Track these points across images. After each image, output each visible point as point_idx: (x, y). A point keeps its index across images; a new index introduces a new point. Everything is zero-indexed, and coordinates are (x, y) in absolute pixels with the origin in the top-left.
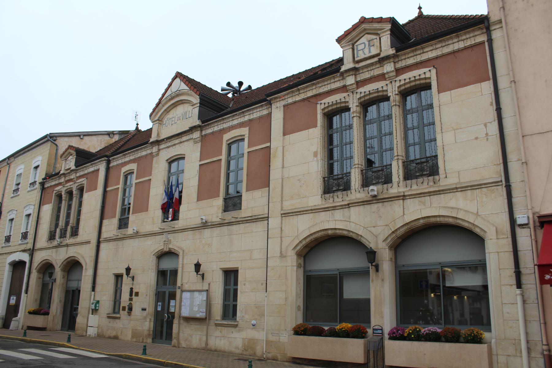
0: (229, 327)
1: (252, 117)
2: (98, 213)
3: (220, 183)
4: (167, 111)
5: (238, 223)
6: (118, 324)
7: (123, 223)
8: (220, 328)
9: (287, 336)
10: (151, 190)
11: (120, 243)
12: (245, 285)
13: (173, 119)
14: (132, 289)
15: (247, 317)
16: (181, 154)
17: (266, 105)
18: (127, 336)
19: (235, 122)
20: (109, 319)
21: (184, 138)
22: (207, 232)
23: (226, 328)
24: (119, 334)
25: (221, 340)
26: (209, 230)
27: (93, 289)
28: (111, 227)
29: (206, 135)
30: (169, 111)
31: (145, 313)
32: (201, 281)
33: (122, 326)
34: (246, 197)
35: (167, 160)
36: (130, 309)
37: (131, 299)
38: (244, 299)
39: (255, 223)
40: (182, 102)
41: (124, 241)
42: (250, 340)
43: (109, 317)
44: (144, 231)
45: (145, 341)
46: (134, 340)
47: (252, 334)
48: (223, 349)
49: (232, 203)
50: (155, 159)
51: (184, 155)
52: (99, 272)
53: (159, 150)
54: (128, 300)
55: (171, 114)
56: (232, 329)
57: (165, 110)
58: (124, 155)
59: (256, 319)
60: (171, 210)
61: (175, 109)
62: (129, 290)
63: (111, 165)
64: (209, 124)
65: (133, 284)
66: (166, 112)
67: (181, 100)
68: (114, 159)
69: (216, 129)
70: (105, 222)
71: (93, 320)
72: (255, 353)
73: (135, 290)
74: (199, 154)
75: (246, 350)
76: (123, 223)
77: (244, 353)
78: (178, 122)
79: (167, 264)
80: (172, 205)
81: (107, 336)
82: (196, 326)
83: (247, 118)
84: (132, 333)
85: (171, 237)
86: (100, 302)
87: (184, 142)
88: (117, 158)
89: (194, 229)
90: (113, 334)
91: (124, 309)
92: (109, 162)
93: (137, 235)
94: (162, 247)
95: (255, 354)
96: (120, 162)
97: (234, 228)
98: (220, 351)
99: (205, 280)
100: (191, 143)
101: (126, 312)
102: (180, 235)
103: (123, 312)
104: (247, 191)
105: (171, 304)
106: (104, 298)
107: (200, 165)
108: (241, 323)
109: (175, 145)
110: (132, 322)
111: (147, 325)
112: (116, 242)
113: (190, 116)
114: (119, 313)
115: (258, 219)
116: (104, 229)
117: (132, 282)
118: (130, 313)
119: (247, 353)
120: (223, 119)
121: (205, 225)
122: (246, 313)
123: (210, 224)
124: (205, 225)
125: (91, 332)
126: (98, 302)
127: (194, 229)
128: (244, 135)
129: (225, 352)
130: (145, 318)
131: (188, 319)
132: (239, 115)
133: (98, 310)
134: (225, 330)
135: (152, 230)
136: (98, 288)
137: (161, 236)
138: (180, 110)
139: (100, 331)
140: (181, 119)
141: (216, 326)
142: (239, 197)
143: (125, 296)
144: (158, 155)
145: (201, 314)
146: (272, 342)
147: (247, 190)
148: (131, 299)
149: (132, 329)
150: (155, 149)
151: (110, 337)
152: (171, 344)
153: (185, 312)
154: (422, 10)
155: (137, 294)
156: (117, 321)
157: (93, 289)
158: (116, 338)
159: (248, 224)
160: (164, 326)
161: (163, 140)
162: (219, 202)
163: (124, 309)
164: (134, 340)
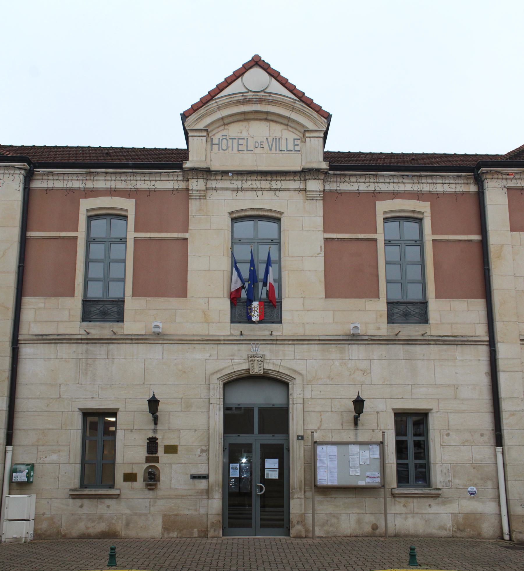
0: (424, 498)
1: (439, 188)
2: (11, 280)
3: (377, 276)
4: (225, 122)
5: (427, 342)
7: (103, 310)
8: (402, 500)
11: (100, 350)
13: (241, 142)
15: (457, 481)
16: (271, 211)
17: (467, 179)
18: (155, 529)
19: (409, 187)
20: (79, 502)
22: (357, 352)
23: (415, 500)
24: (119, 527)
25: (406, 518)
26: (362, 347)
27: (9, 440)
28: (55, 313)
29: (331, 191)
30: (228, 124)
31: (202, 484)
32: (352, 427)
33: (128, 511)
34: (436, 307)
35: (231, 213)
36: (152, 478)
38: (444, 454)
39: (459, 347)
40: (266, 117)
41: (111, 346)
43: (74, 497)
44: (180, 332)
45: (211, 533)
46: (175, 534)
47: (470, 506)
48: (412, 531)
49: (408, 311)
50: (194, 205)
51: (281, 213)
52: (21, 404)
53: (207, 189)
54: (144, 460)
55: (234, 130)
56: (430, 501)
57: (222, 118)
59: (475, 485)
60: (255, 304)
61: (245, 124)
62: (145, 443)
63: (36, 184)
64: (346, 175)
65: (155, 431)
66: (221, 123)
67: (267, 113)
68: (49, 173)
69: (363, 187)
70: (28, 301)
72: (479, 534)
74: (319, 221)
75: (462, 531)
76: (103, 310)
77: (459, 534)
78: (258, 151)
80: (255, 296)
82: (346, 500)
83: (426, 188)
84: (163, 522)
85: (263, 350)
86: (36, 467)
88: (58, 174)
89: (324, 342)
90: (101, 527)
91: (130, 477)
92: (29, 177)
93: (157, 338)
94: (245, 366)
95: (479, 535)
96: (77, 185)
97: (418, 349)
98: (406, 536)
99: (360, 427)
100: (299, 197)
101: (140, 482)
102: (289, 349)
104: (438, 296)
105: (267, 466)
107: (326, 240)
108: (445, 491)
110: (161, 503)
111: (216, 504)
112: (85, 347)
113: (291, 147)
115: (468, 341)
116: (27, 315)
117: (153, 426)
118: (155, 485)
119: (464, 534)
121: (354, 339)
122: (454, 476)
123: (367, 338)
124: (354, 339)
126: (31, 467)
127: (324, 342)
128: (422, 213)
129: (417, 536)
130: (208, 492)
131: (327, 491)
132: (411, 179)
133: (32, 482)
134: (414, 504)
135: (207, 333)
136: (19, 437)
137: (235, 347)
138: (259, 130)
139: (44, 526)
140: (266, 146)
141: (394, 497)
142: (425, 304)
144: (203, 197)
147: (438, 297)
149: (164, 516)
150: (197, 184)
152: (288, 534)
153: (327, 476)
155: (171, 449)
156: (108, 502)
157: (9, 440)
159: (445, 347)
160: (256, 503)
161: (225, 173)
162: (381, 305)
163: (130, 477)
164: (175, 534)
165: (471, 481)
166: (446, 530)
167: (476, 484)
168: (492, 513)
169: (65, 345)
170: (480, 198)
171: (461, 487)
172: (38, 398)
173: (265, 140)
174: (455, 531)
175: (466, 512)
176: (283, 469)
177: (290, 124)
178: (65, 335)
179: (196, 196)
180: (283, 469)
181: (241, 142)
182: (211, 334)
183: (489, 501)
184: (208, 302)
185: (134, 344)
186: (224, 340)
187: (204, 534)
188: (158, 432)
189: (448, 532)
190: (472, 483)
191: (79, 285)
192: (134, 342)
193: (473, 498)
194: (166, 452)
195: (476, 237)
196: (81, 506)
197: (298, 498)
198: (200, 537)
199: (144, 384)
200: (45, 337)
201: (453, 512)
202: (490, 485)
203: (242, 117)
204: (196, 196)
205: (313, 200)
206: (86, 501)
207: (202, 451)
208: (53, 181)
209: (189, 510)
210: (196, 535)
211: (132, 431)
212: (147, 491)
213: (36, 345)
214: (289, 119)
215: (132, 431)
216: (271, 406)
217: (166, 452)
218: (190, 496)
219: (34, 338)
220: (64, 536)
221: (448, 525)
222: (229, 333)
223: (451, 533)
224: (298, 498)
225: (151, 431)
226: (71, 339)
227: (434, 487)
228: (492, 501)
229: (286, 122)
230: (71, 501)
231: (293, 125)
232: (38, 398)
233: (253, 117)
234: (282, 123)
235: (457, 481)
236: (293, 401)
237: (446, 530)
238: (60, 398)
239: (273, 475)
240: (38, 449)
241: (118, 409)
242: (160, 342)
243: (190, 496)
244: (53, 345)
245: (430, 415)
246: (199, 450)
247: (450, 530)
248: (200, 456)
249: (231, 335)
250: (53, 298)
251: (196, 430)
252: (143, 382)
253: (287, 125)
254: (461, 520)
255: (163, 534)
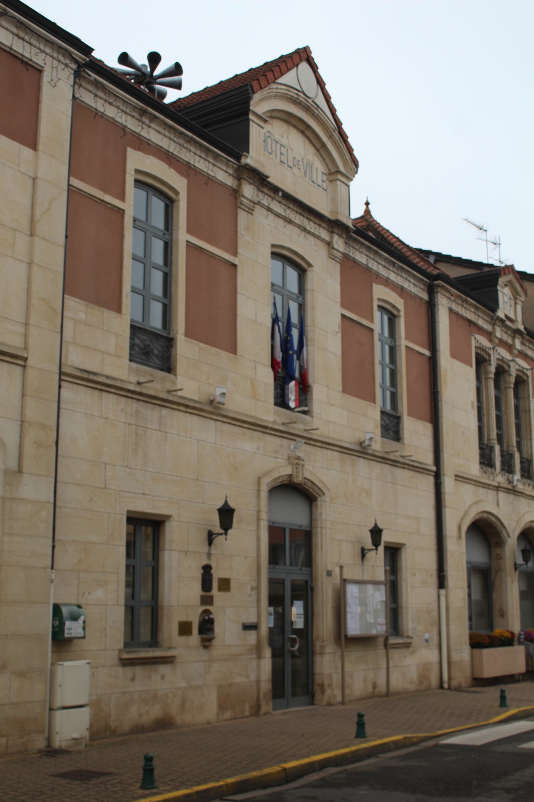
6: (164, 682)
10: (240, 299)
11: (152, 414)
12: (415, 575)
14: (207, 570)
16: (303, 258)
17: (424, 285)
20: (129, 671)
21: (311, 226)
26: (366, 462)
31: (252, 637)
32: (360, 562)
33: (183, 684)
35: (273, 246)
37: (207, 600)
41: (165, 411)
46: (228, 715)
51: (310, 265)
54: (198, 601)
58: (143, 112)
59: (428, 632)
65: (209, 555)
67: (308, 127)
71: (75, 679)
73: (217, 574)
79: (293, 514)
81: (126, 726)
84: (219, 697)
87: (309, 232)
89: (343, 450)
91: (185, 629)
94: (288, 470)
97: (399, 472)
103: (183, 639)
106: (99, 594)
109: (290, 222)
114: (154, 641)
120: (376, 253)
125: (71, 727)
127: (343, 450)
137: (278, 440)
143: (180, 591)
145: (379, 628)
148: (207, 600)
151: (138, 730)
154: (370, 206)
155: (225, 585)
158: (164, 724)
159: (413, 473)
163: (185, 629)
169: (112, 396)
170: (431, 307)
172: (78, 485)
173: (301, 160)
176: (309, 614)
177: (321, 151)
178: (115, 379)
179: (246, 206)
180: (309, 614)
181: (283, 150)
182: (259, 416)
184: (255, 368)
185: (188, 415)
186: (272, 429)
187: (256, 710)
188: (213, 557)
191: (127, 296)
192: (189, 410)
194: (220, 589)
195: (427, 353)
196: (133, 679)
197: (329, 653)
198: (251, 715)
199: (197, 479)
200: (92, 377)
203: (286, 117)
204: (246, 206)
205: (334, 259)
206: (138, 670)
207: (253, 589)
208: (103, 102)
209: (241, 675)
210: (247, 713)
211: (186, 553)
212: (202, 651)
213: (75, 386)
214: (324, 145)
215: (186, 553)
216: (298, 528)
217: (220, 589)
218: (242, 655)
219: (79, 374)
220: (114, 733)
222: (272, 419)
224: (329, 653)
225: (206, 555)
226: (121, 389)
227: (405, 635)
229: (318, 146)
230: (120, 670)
231: (323, 154)
232: (78, 485)
233: (294, 122)
234: (314, 145)
236: (322, 523)
238: (105, 488)
239: (299, 624)
240: (79, 579)
241: (169, 517)
242: (214, 417)
243: (242, 655)
244: (97, 392)
245: (403, 551)
246: (249, 587)
248: (250, 596)
249: (275, 422)
250: (97, 308)
251: (246, 557)
252: (196, 478)
253: (318, 150)
255: (218, 715)
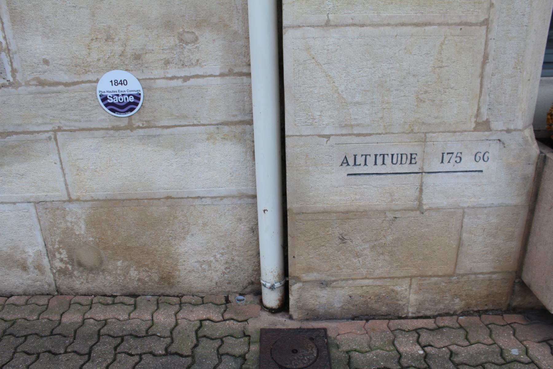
9: (492, 167)
42: (107, 209)
59: (136, 61)
72: (167, 279)
77: (80, 282)
146: (347, 215)
165: (109, 38)
166: (25, 268)
167: (137, 57)
168: (223, 191)
171: (65, 78)
174: (63, 272)
175: (101, 194)
183: (210, 137)
189: (33, 274)
190: (118, 48)
193: (130, 127)
201: (41, 195)
202: (211, 52)
221: (31, 251)
223: (49, 278)
228: (225, 138)
235: (37, 46)
237: (25, 268)
247: (39, 268)
254: (81, 229)
